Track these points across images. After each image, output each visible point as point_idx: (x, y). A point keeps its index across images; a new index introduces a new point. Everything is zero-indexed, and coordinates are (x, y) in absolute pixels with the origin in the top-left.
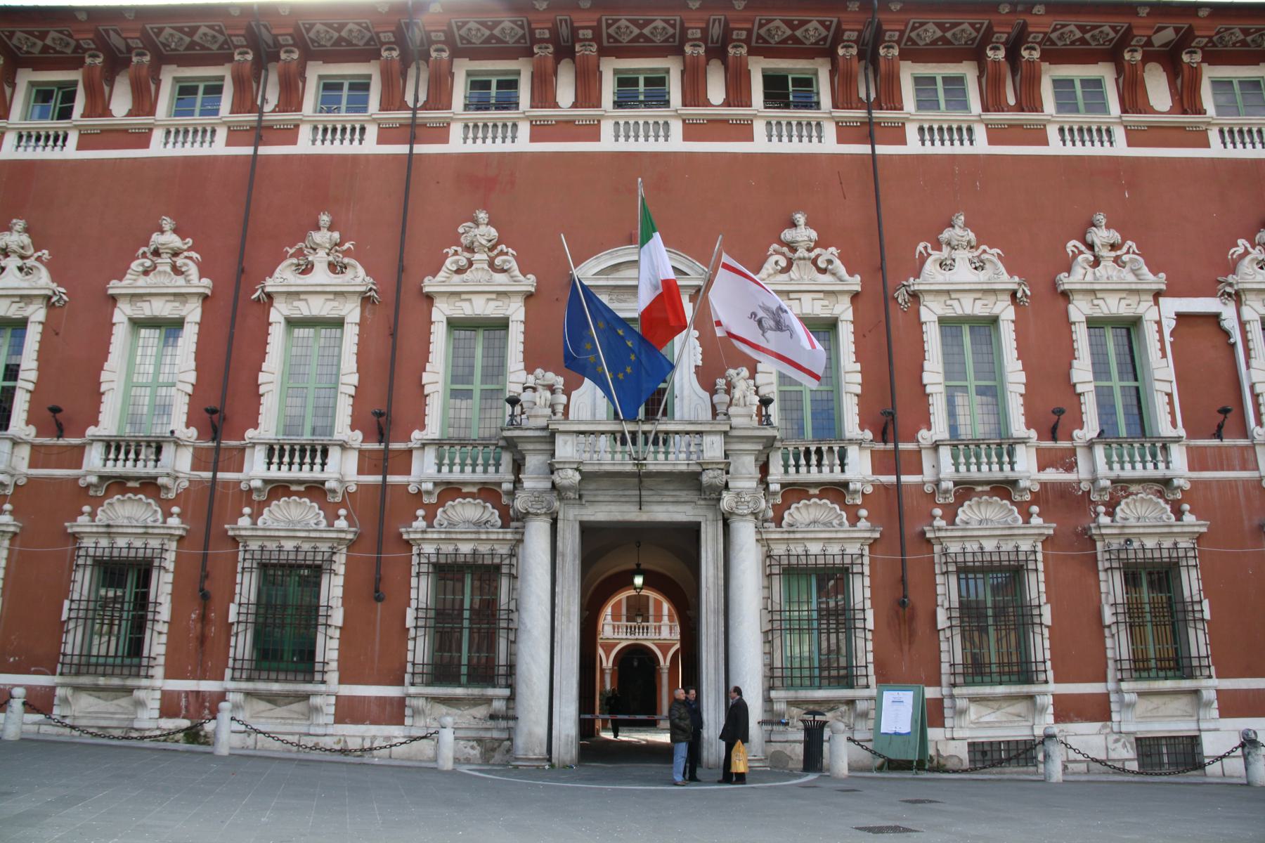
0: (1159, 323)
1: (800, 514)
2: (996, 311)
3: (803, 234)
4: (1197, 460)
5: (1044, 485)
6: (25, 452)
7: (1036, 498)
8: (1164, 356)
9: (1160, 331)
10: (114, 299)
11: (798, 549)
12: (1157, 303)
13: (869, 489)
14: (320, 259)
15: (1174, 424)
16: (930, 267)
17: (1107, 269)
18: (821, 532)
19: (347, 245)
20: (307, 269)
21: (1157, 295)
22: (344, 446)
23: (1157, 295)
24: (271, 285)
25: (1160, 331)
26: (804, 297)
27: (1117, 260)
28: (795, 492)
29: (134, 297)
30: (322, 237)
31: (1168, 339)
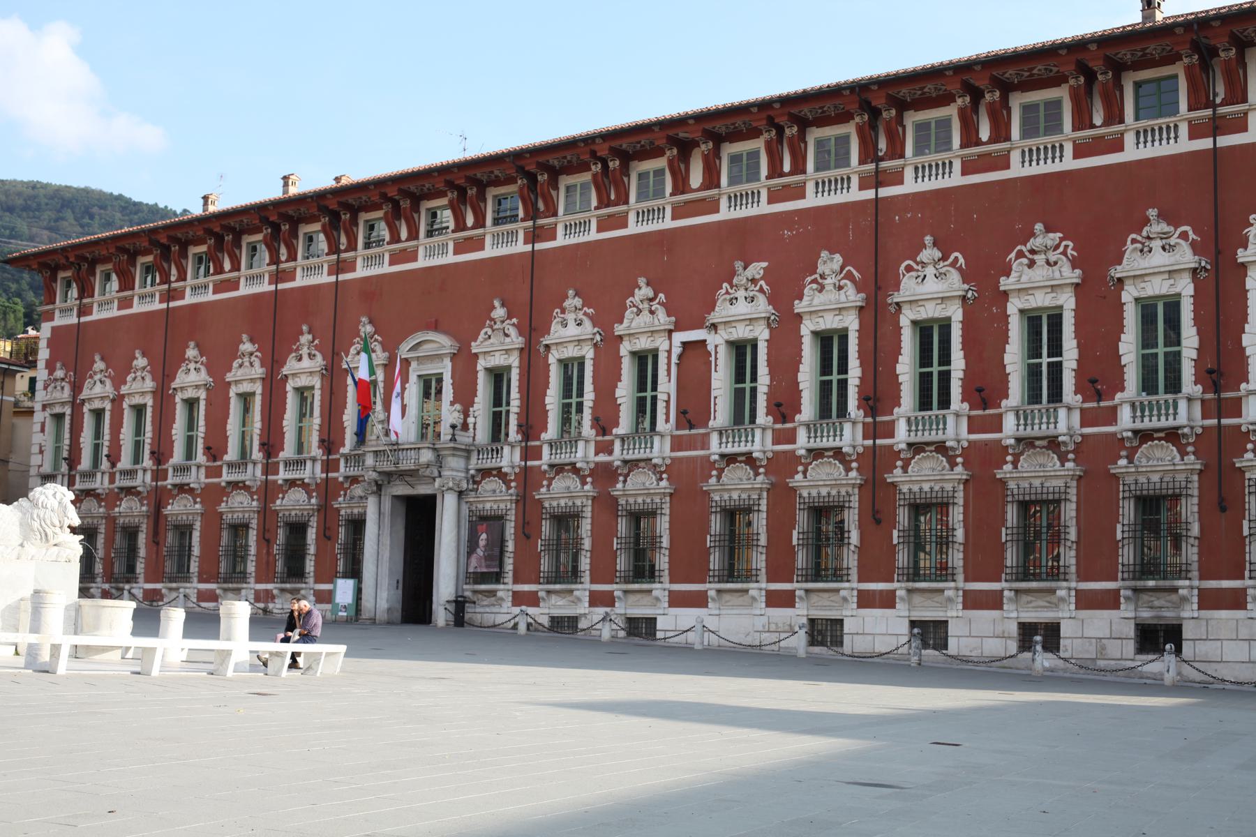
0: (669, 352)
1: (491, 485)
2: (583, 353)
3: (499, 312)
4: (677, 444)
5: (597, 464)
6: (203, 471)
7: (593, 473)
8: (669, 374)
9: (669, 358)
10: (229, 383)
11: (480, 506)
12: (670, 338)
13: (517, 470)
14: (305, 351)
15: (667, 421)
16: (555, 327)
17: (645, 317)
18: (496, 497)
19: (316, 342)
20: (300, 359)
21: (670, 332)
22: (314, 460)
23: (670, 332)
24: (285, 371)
25: (669, 358)
26: (497, 354)
27: (652, 312)
28: (486, 473)
29: (237, 382)
30: (305, 338)
31: (674, 359)
